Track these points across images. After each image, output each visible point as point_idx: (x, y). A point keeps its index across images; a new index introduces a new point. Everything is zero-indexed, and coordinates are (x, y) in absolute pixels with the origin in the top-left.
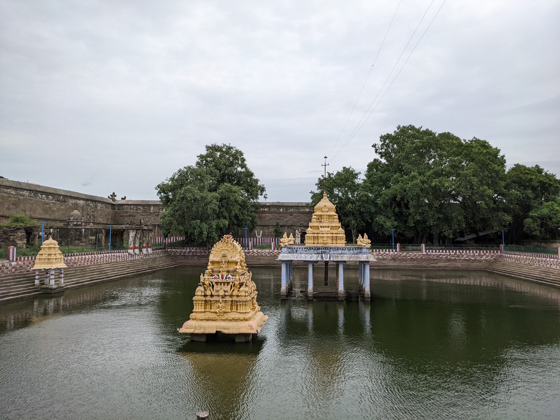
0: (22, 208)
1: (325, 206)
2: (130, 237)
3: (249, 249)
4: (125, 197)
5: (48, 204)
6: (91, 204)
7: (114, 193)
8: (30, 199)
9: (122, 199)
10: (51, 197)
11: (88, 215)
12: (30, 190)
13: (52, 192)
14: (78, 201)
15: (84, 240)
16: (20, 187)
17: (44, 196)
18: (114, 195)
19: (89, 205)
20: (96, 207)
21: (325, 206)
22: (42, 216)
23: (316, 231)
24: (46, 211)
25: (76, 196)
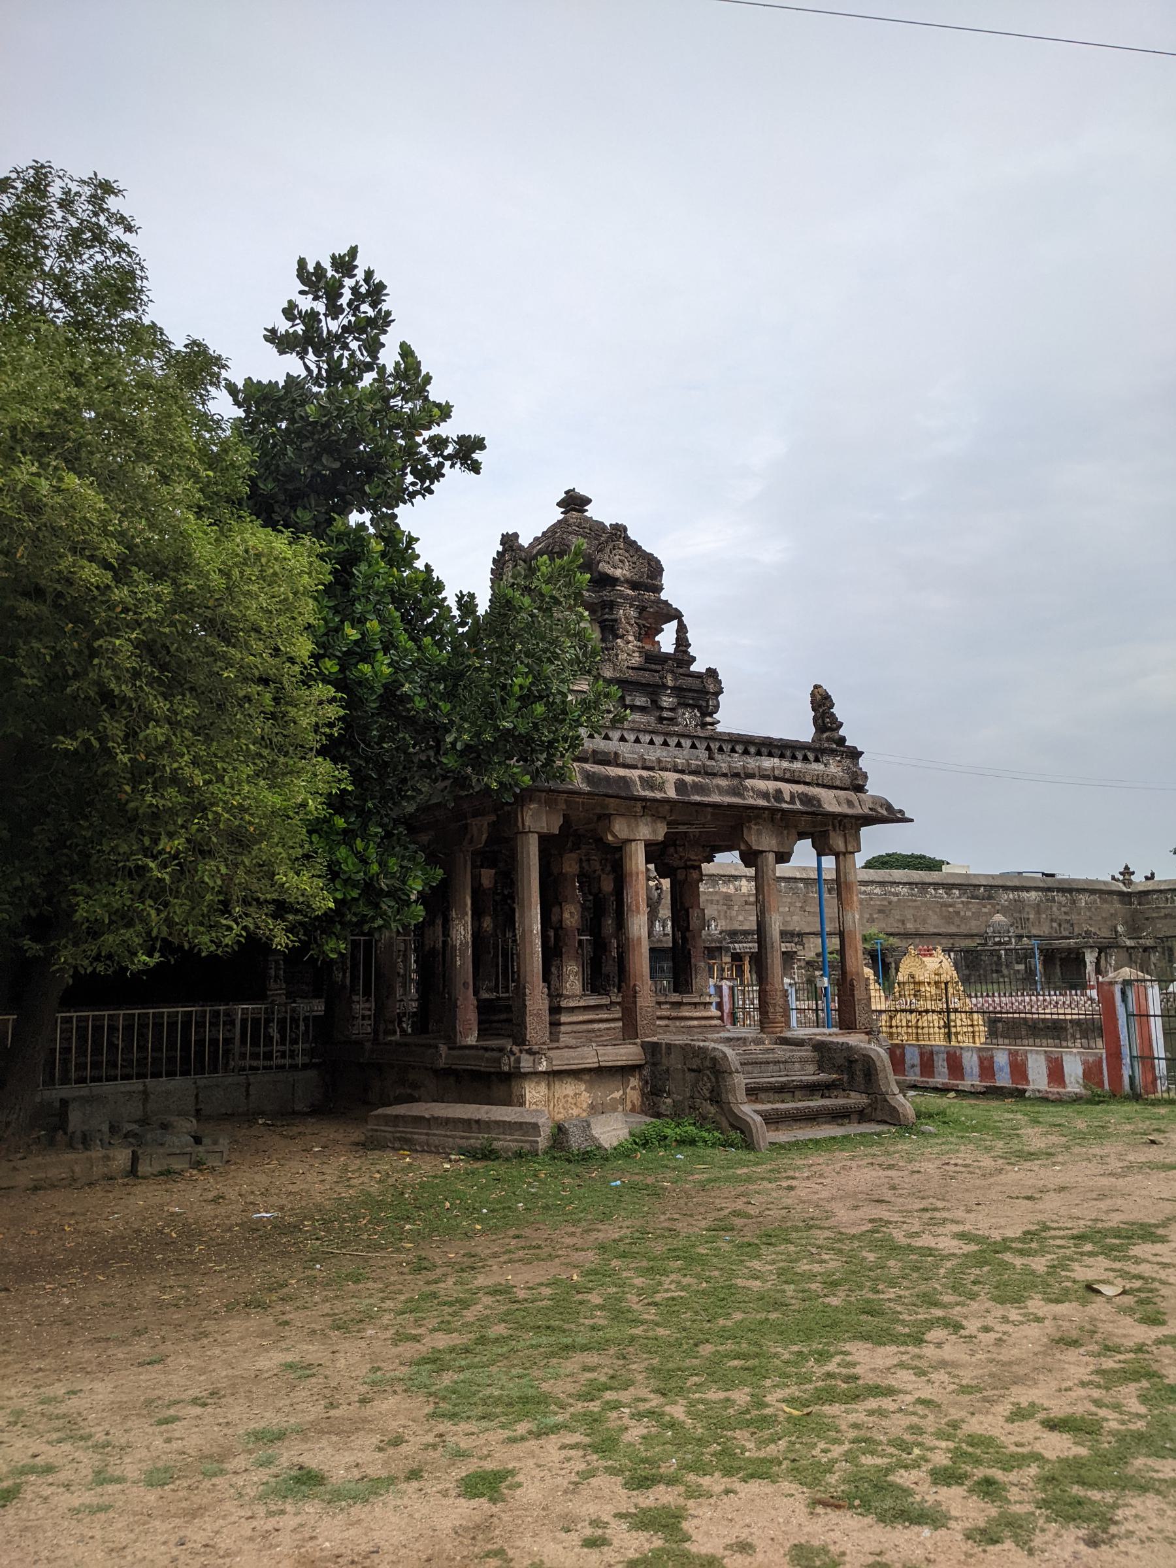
2: (1088, 963)
4: (1153, 874)
6: (1060, 898)
7: (1127, 868)
9: (1147, 878)
10: (957, 892)
11: (1052, 920)
12: (910, 884)
13: (958, 881)
14: (1024, 895)
15: (1005, 972)
16: (891, 879)
18: (1127, 872)
19: (1053, 901)
20: (1074, 902)
24: (948, 920)
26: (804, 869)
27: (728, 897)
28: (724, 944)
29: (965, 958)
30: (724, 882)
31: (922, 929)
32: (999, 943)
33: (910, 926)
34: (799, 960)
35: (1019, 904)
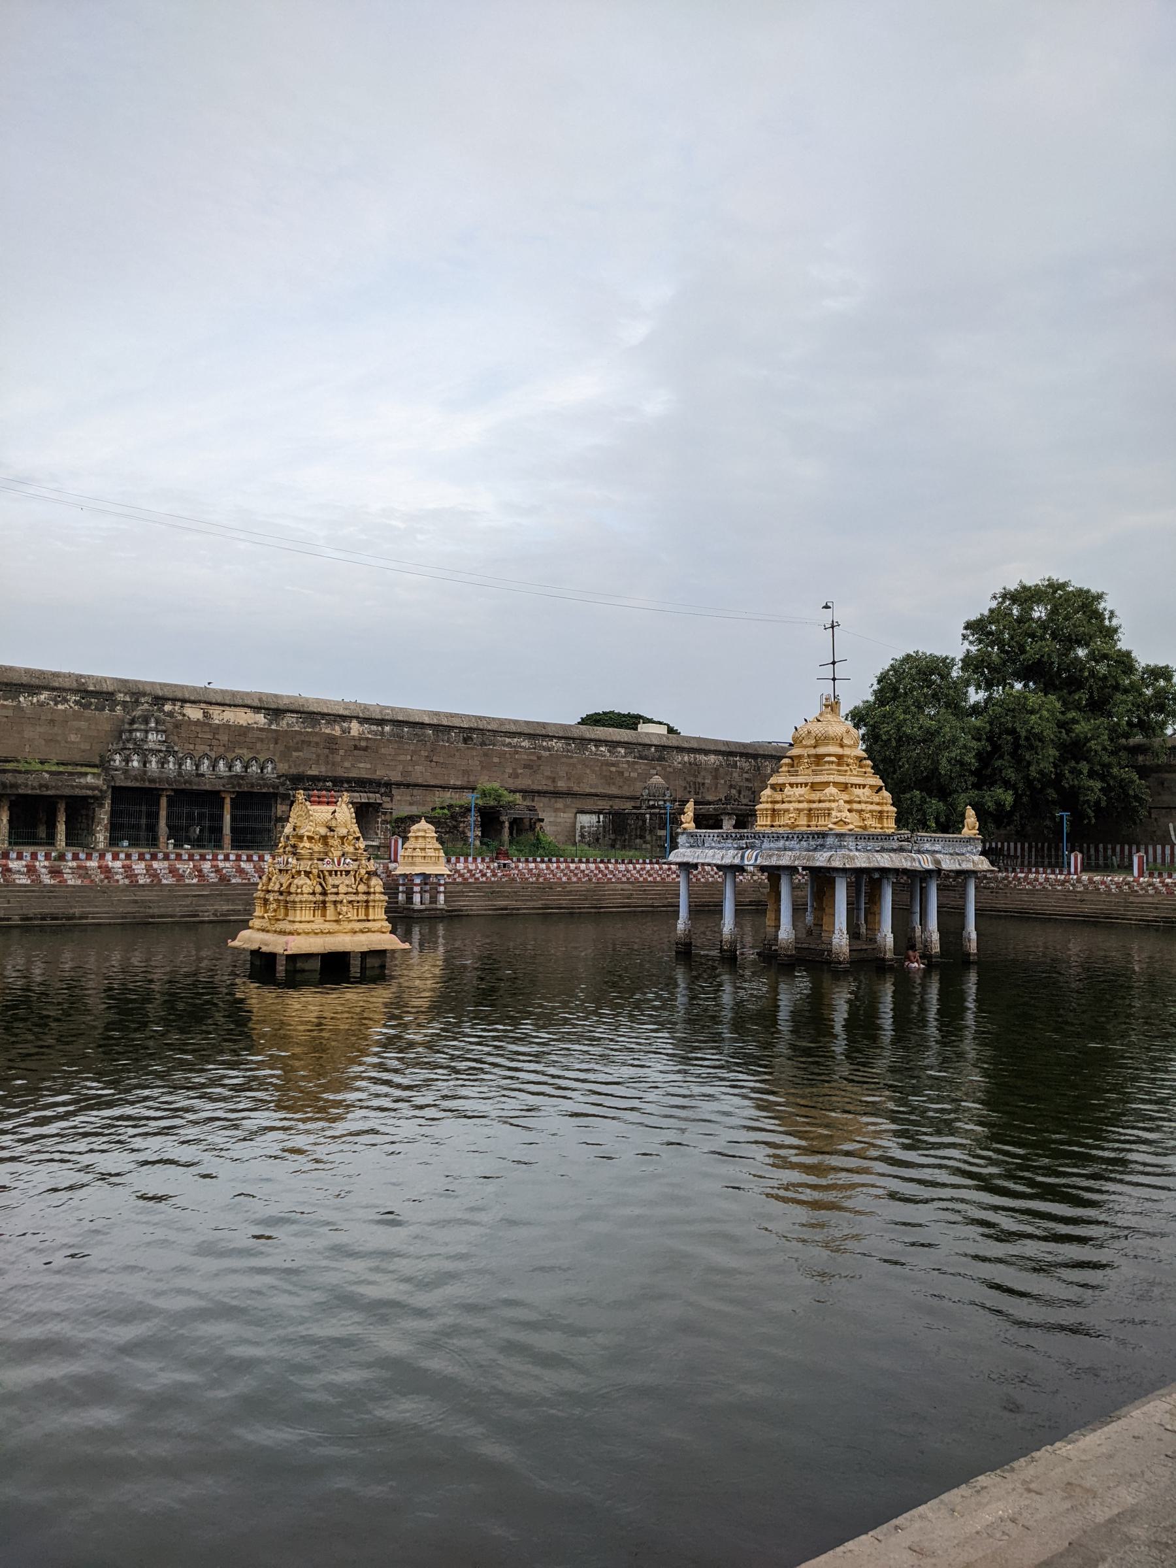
0: (548, 774)
1: (809, 732)
3: (1069, 873)
5: (613, 765)
6: (742, 763)
8: (566, 756)
10: (623, 751)
11: (731, 787)
14: (702, 758)
15: (648, 838)
16: (544, 732)
17: (603, 749)
19: (735, 766)
21: (809, 732)
22: (600, 790)
23: (778, 797)
24: (609, 780)
25: (695, 745)
26: (437, 714)
27: (331, 739)
28: (282, 790)
29: (613, 822)
30: (328, 722)
31: (576, 789)
32: (653, 807)
33: (562, 785)
34: (385, 813)
35: (695, 768)
